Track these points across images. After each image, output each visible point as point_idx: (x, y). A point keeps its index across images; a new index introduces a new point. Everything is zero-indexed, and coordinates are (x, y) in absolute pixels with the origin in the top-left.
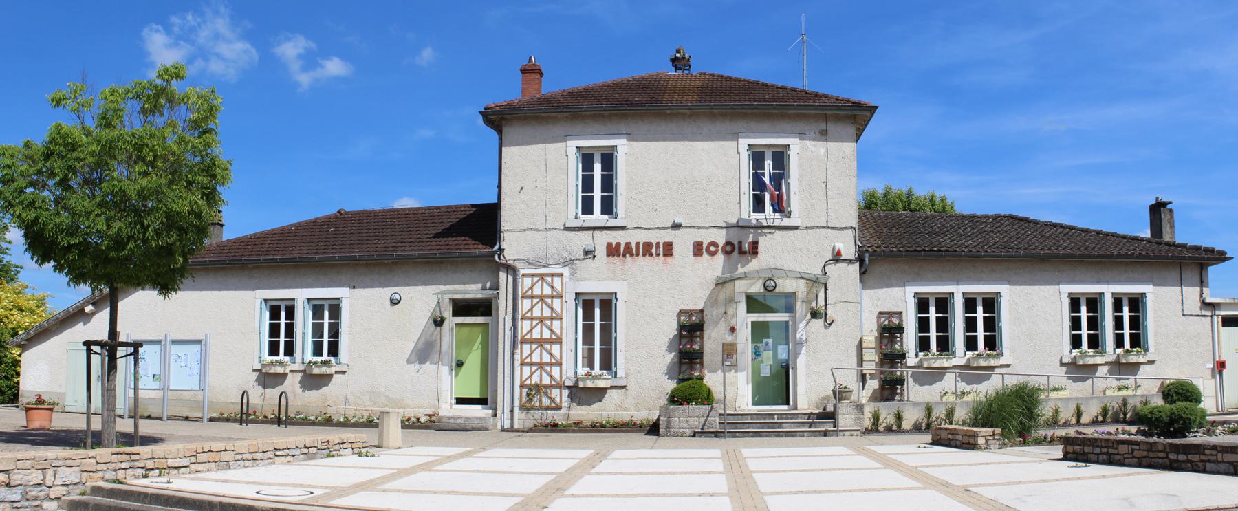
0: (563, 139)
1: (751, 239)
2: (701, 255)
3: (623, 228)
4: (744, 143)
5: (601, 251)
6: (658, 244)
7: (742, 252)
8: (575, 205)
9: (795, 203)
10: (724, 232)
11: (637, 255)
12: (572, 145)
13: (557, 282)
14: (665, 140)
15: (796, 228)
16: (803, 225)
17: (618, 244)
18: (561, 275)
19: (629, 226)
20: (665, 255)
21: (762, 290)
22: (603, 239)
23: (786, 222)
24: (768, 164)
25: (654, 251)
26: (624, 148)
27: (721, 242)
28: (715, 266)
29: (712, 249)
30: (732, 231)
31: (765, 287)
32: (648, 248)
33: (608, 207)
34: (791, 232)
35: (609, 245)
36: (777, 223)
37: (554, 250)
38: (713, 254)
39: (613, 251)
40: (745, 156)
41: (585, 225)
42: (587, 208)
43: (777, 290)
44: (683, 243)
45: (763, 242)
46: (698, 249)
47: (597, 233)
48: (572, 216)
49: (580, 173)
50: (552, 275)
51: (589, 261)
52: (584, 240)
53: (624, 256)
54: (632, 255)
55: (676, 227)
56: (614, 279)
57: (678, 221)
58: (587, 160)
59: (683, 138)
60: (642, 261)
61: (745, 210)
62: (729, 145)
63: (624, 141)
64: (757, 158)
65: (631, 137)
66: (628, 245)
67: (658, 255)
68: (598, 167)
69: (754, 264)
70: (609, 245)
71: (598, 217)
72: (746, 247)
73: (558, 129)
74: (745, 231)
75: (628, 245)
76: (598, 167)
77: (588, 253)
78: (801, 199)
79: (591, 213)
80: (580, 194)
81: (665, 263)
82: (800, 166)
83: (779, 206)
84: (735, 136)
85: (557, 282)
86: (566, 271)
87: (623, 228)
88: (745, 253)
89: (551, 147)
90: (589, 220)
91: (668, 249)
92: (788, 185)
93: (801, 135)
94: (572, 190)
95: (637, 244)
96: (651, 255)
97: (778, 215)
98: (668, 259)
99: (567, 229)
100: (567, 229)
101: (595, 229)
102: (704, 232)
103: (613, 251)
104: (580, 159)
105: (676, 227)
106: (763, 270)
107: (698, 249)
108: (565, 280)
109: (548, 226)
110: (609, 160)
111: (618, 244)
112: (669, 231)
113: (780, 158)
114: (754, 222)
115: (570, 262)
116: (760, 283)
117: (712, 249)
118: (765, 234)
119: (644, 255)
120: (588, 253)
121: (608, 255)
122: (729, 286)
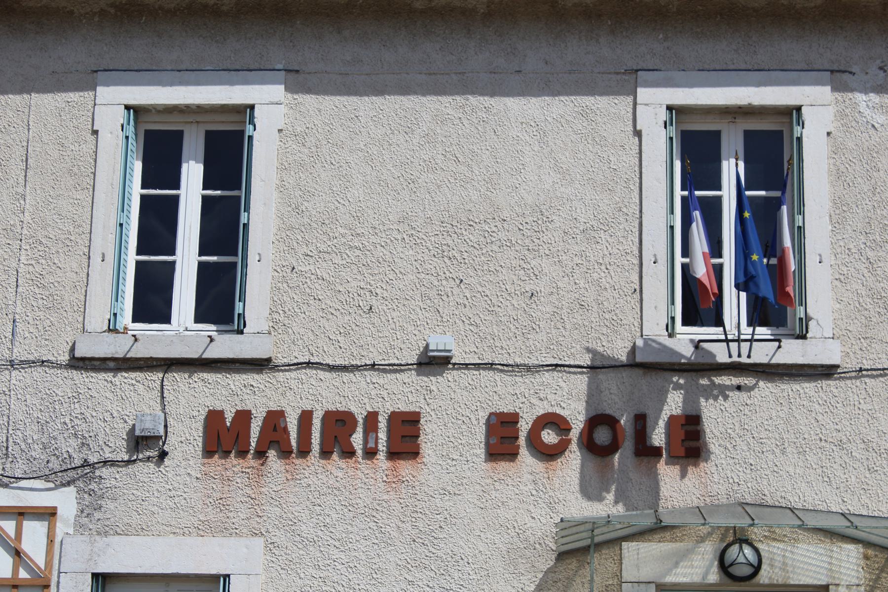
0: (87, 79)
1: (674, 403)
2: (512, 455)
3: (260, 365)
4: (655, 101)
5: (186, 437)
6: (372, 419)
7: (646, 452)
8: (109, 291)
9: (822, 295)
10: (581, 382)
11: (304, 452)
12: (112, 103)
13: (33, 537)
14: (405, 90)
15: (827, 372)
16: (850, 364)
17: (243, 417)
18: (49, 514)
19: (280, 360)
20: (393, 455)
21: (714, 577)
22: (192, 400)
23: (792, 352)
24: (732, 170)
25: (357, 440)
26: (271, 107)
27: (576, 415)
28: (557, 494)
29: (549, 437)
30: (609, 381)
31: (724, 567)
32: (339, 425)
33: (219, 300)
34: (808, 387)
35: (214, 418)
36: (762, 354)
37: (32, 432)
38: (549, 454)
39: (224, 437)
40: (658, 141)
41: (140, 351)
42: (152, 301)
43: (765, 576)
44: (454, 415)
45: (715, 416)
46: (501, 437)
47: (178, 380)
48: (98, 319)
49: (136, 190)
50: (21, 514)
51: (144, 470)
52: (133, 400)
53: (261, 454)
54: (285, 453)
55: (432, 363)
56: (226, 530)
57: (439, 342)
58: (160, 154)
59: (465, 86)
60: (319, 474)
61: (657, 321)
62: (608, 108)
63: (277, 91)
64: (697, 153)
65: (298, 80)
66: (275, 419)
67: (370, 454)
68: (192, 174)
69: (677, 489)
70: (214, 418)
71: (184, 329)
72: (658, 437)
73: (73, 51)
74: (656, 380)
75: (275, 419)
76: (192, 174)
77: (145, 445)
78: (842, 279)
79: (167, 319)
80: (132, 257)
81: (394, 481)
82: (837, 175)
83: (774, 306)
84: (626, 81)
85: (33, 537)
86: (66, 501)
87: (260, 365)
88: (656, 452)
89: (46, 103)
90: (154, 339)
91: (405, 436)
92: (799, 233)
93: (840, 77)
94: (104, 240)
95: (306, 417)
96: (349, 453)
97: (763, 332)
98: (405, 467)
99: (79, 363)
100: (79, 363)
101: (169, 365)
102: (523, 384)
103: (224, 437)
104: (136, 149)
105: (432, 363)
106: (716, 508)
107: (501, 437)
108: (62, 528)
109: (19, 353)
110: (228, 156)
111: (243, 417)
112: (410, 377)
113: (772, 151)
114: (687, 351)
115: (81, 473)
116: (707, 552)
117: (549, 437)
118: (723, 391)
119: (325, 454)
120: (145, 445)
121: (208, 452)
122: (601, 561)
